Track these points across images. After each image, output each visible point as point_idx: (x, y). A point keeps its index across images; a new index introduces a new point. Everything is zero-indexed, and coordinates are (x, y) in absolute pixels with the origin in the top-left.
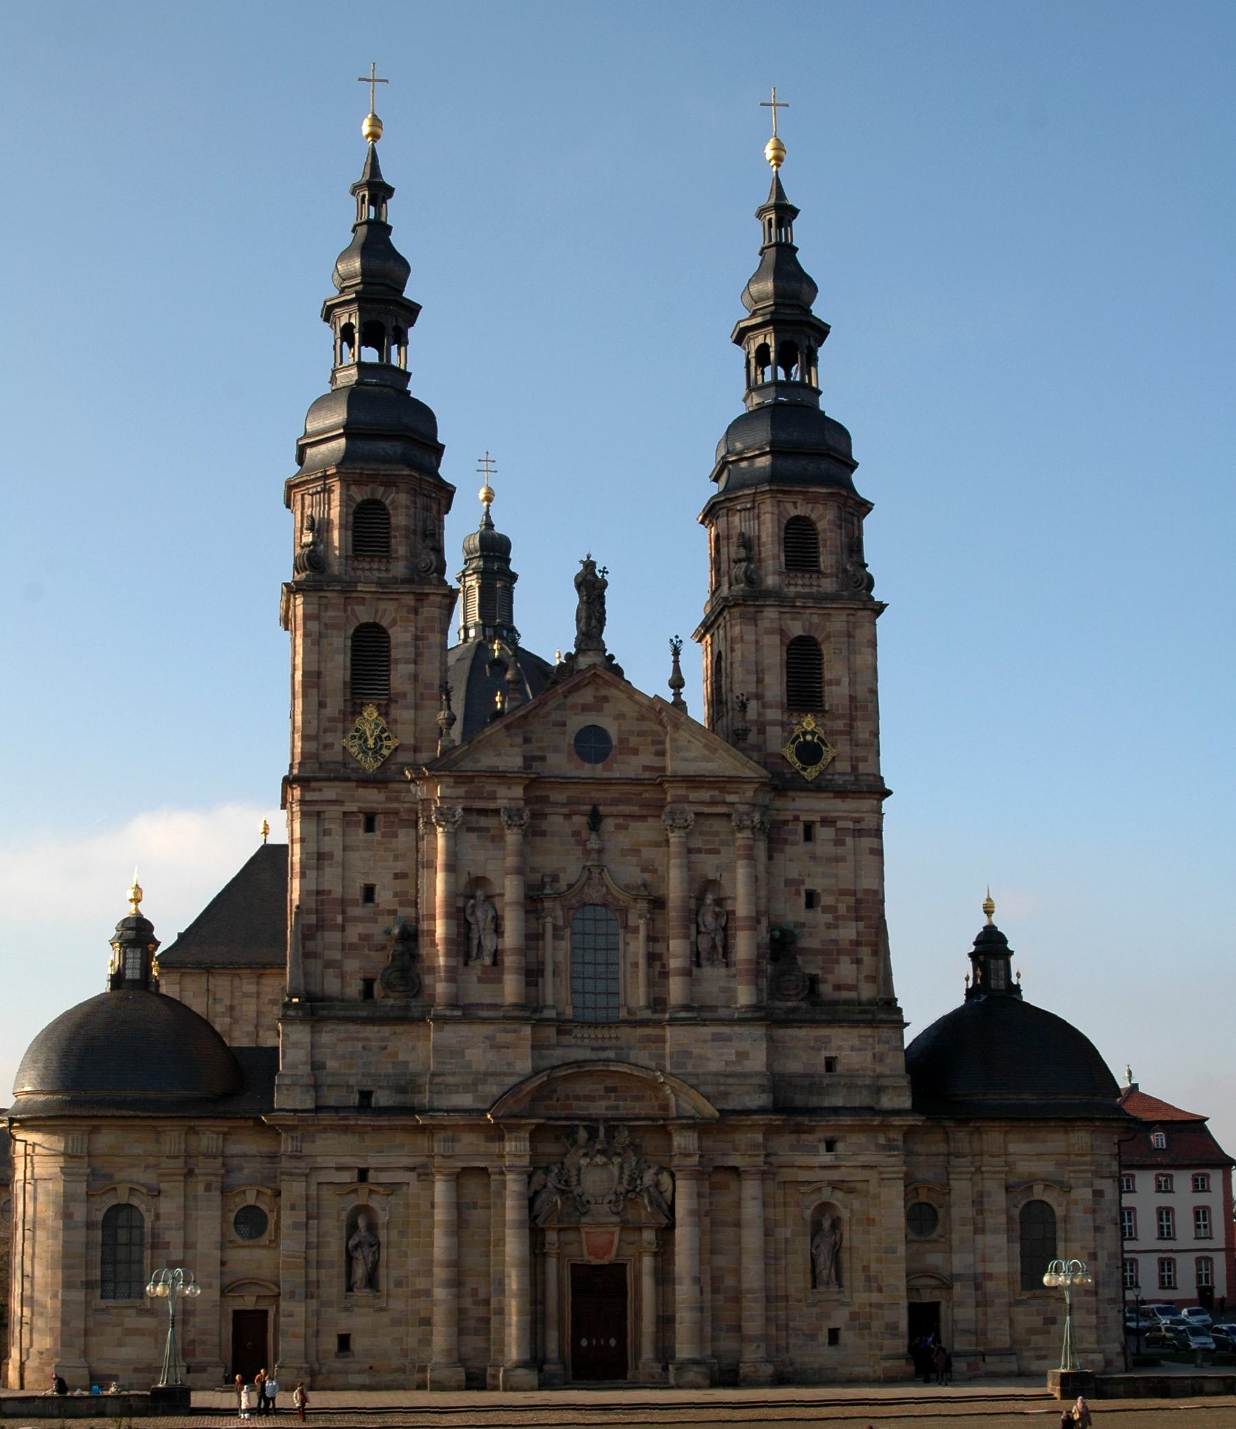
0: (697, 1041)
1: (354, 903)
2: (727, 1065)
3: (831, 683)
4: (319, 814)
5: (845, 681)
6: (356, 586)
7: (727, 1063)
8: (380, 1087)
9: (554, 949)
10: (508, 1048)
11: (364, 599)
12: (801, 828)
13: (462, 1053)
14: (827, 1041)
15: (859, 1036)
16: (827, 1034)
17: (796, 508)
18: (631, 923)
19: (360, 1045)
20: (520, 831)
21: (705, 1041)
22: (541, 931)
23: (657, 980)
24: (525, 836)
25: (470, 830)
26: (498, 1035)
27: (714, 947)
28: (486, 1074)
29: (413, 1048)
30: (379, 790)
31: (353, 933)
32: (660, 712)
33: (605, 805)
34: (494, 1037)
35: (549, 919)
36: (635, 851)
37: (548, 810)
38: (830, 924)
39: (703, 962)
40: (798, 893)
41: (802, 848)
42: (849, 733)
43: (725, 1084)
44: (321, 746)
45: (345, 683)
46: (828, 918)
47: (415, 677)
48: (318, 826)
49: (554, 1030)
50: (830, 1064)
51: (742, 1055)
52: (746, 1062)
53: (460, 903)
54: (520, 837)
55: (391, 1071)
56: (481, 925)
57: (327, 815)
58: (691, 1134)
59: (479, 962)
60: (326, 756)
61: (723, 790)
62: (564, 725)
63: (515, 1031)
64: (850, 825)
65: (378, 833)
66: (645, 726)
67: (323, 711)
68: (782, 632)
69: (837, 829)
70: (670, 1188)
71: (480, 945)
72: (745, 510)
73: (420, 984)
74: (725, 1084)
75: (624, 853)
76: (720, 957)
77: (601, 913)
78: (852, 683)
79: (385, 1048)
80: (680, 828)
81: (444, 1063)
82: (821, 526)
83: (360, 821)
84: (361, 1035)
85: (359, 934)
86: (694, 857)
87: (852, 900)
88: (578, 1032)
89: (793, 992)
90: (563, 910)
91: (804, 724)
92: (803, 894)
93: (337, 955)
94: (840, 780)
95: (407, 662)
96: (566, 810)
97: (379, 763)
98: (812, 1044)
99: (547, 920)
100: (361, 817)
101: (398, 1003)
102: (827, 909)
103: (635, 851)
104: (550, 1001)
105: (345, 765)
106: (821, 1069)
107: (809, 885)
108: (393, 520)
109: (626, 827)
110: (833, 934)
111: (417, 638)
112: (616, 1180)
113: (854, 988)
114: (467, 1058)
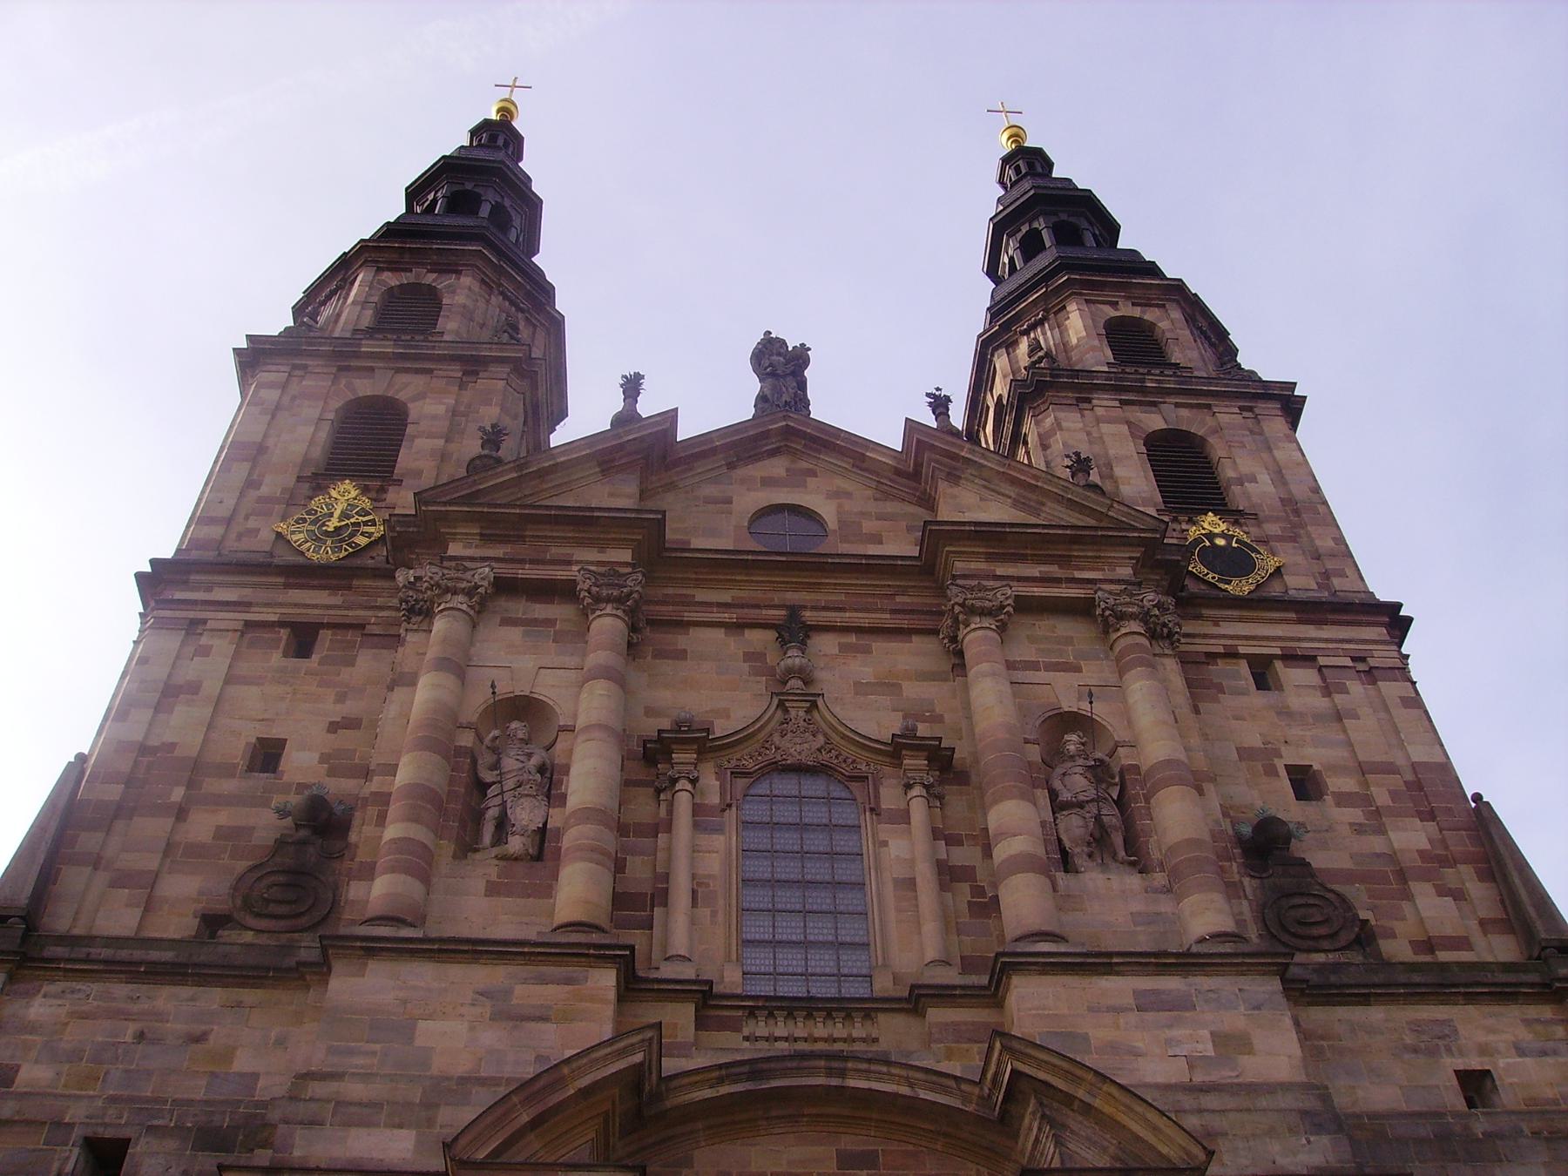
0: (1090, 1009)
1: (227, 771)
2: (1191, 1067)
3: (1240, 482)
4: (194, 623)
5: (1264, 478)
6: (360, 346)
7: (1192, 1062)
8: (151, 1129)
9: (695, 849)
10: (543, 1019)
11: (372, 369)
12: (1244, 668)
13: (406, 1030)
14: (1441, 1039)
15: (1527, 1022)
16: (1446, 1017)
17: (1117, 310)
18: (890, 797)
19: (131, 1028)
20: (619, 613)
21: (1118, 1010)
22: (663, 812)
23: (965, 918)
24: (633, 628)
25: (508, 622)
26: (519, 990)
27: (1099, 841)
28: (463, 1080)
29: (281, 1042)
30: (333, 589)
31: (202, 826)
32: (915, 475)
33: (814, 608)
34: (508, 992)
35: (683, 784)
36: (888, 685)
37: (689, 616)
38: (1360, 825)
39: (1078, 861)
40: (1271, 772)
41: (1258, 699)
42: (1294, 539)
43: (1200, 1111)
44: (233, 536)
45: (306, 461)
46: (1354, 814)
47: (443, 457)
48: (183, 644)
49: (690, 1009)
50: (1475, 1084)
51: (1230, 1044)
52: (1244, 1060)
53: (466, 739)
54: (620, 625)
55: (200, 1095)
56: (509, 784)
57: (210, 625)
59: (495, 851)
60: (231, 543)
61: (1064, 561)
62: (729, 501)
63: (568, 981)
64: (1348, 662)
65: (315, 657)
66: (890, 507)
67: (253, 494)
68: (1129, 423)
69: (1320, 669)
71: (502, 824)
72: (1033, 327)
73: (335, 903)
74: (1200, 1111)
75: (861, 688)
76: (1122, 854)
77: (814, 786)
78: (1279, 476)
79: (200, 1038)
80: (984, 613)
81: (351, 1052)
82: (1164, 325)
83: (280, 640)
84: (135, 1008)
85: (219, 828)
86: (1020, 676)
87: (1395, 781)
88: (762, 1029)
89: (1322, 931)
90: (719, 776)
91: (1206, 525)
92: (1283, 773)
93: (153, 863)
94: (1303, 596)
95: (431, 436)
96: (725, 616)
97: (343, 554)
98: (1408, 1041)
99: (678, 786)
100: (284, 633)
101: (264, 940)
102: (1343, 799)
103: (888, 685)
104: (679, 944)
105: (271, 554)
106: (1457, 1101)
107: (1291, 757)
108: (445, 301)
109: (867, 651)
110: (1376, 844)
111: (454, 413)
113: (1463, 943)
114: (419, 1042)
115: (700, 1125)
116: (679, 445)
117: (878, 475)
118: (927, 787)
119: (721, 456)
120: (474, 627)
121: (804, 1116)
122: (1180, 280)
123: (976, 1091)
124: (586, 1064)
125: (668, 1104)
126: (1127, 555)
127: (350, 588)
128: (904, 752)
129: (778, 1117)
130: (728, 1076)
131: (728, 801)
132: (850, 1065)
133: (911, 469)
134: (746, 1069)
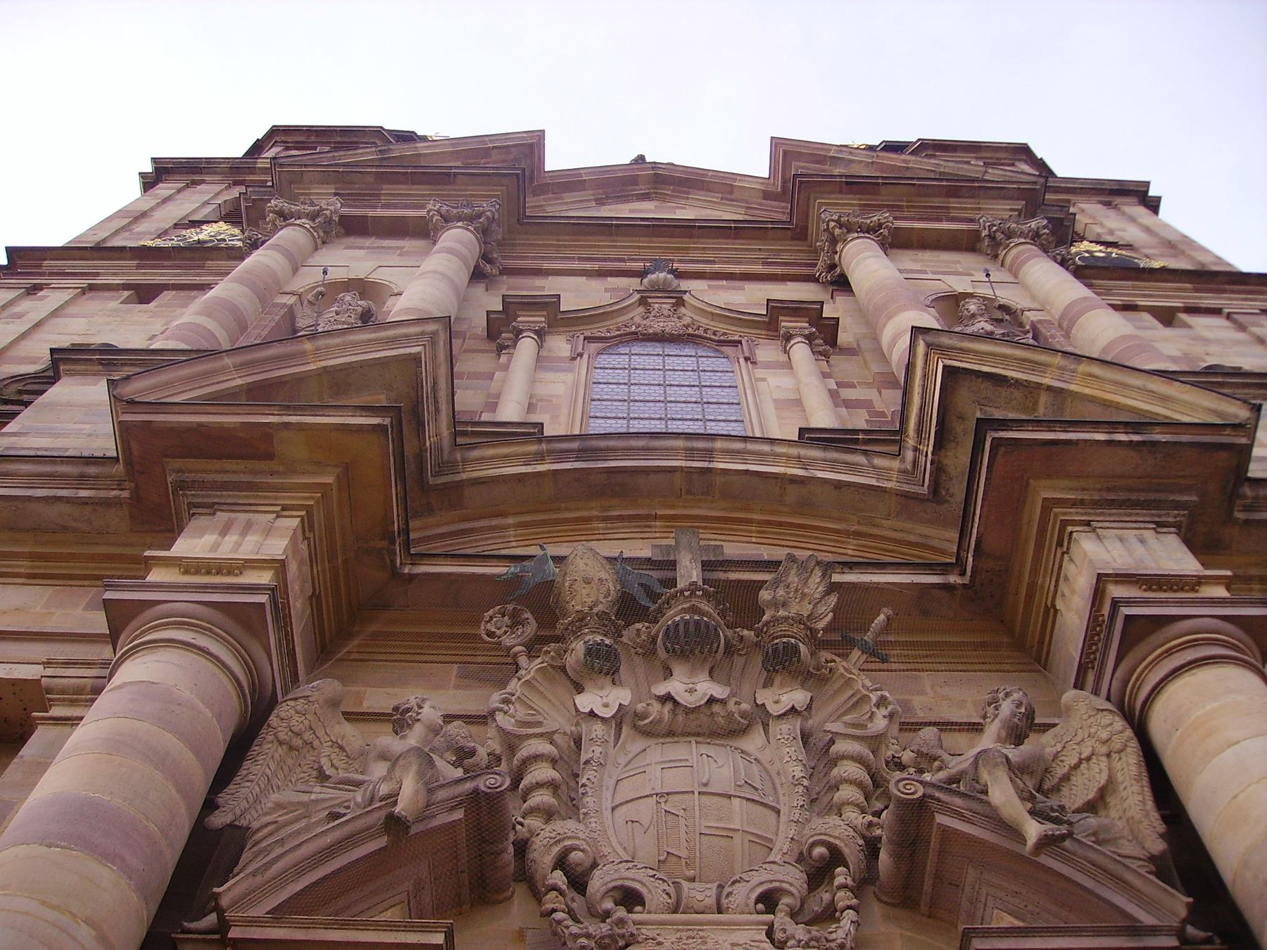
58: (1149, 535)
65: (152, 304)
70: (1130, 764)
112: (790, 802)
115: (510, 520)
116: (547, 175)
117: (747, 202)
118: (806, 337)
119: (590, 192)
120: (316, 249)
121: (656, 517)
122: (1026, 144)
123: (895, 464)
124: (338, 345)
125: (464, 476)
126: (1009, 207)
127: (202, 267)
128: (781, 318)
129: (621, 518)
130: (550, 452)
131: (580, 350)
132: (719, 444)
133: (779, 190)
134: (575, 445)
